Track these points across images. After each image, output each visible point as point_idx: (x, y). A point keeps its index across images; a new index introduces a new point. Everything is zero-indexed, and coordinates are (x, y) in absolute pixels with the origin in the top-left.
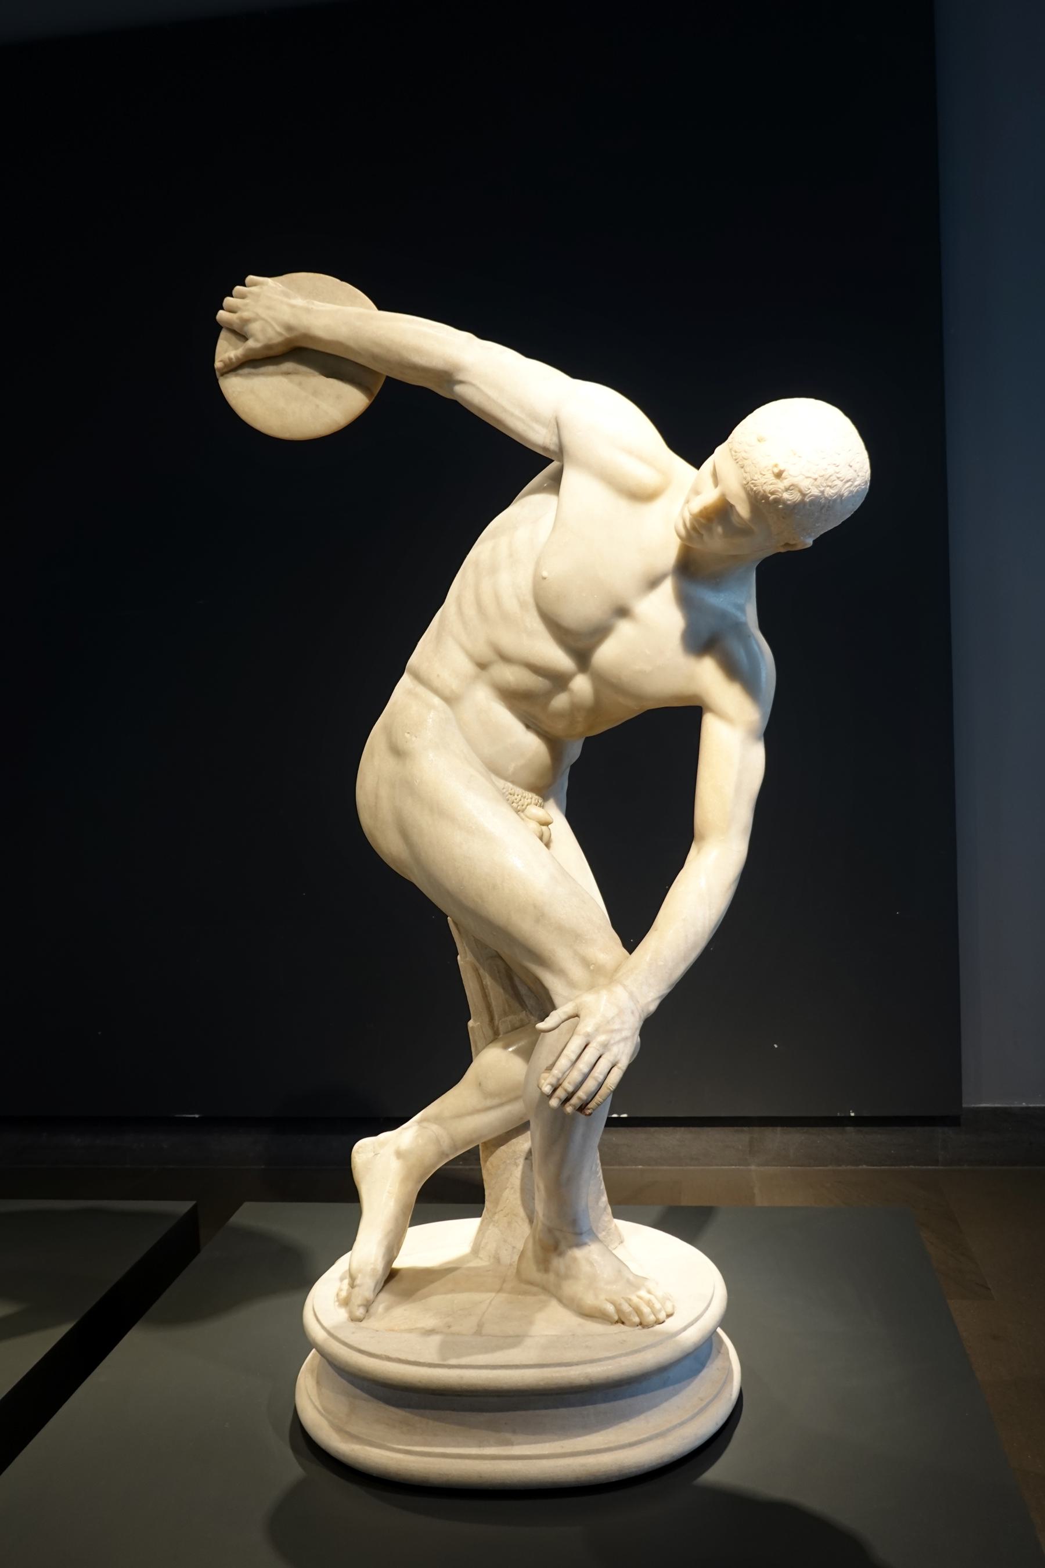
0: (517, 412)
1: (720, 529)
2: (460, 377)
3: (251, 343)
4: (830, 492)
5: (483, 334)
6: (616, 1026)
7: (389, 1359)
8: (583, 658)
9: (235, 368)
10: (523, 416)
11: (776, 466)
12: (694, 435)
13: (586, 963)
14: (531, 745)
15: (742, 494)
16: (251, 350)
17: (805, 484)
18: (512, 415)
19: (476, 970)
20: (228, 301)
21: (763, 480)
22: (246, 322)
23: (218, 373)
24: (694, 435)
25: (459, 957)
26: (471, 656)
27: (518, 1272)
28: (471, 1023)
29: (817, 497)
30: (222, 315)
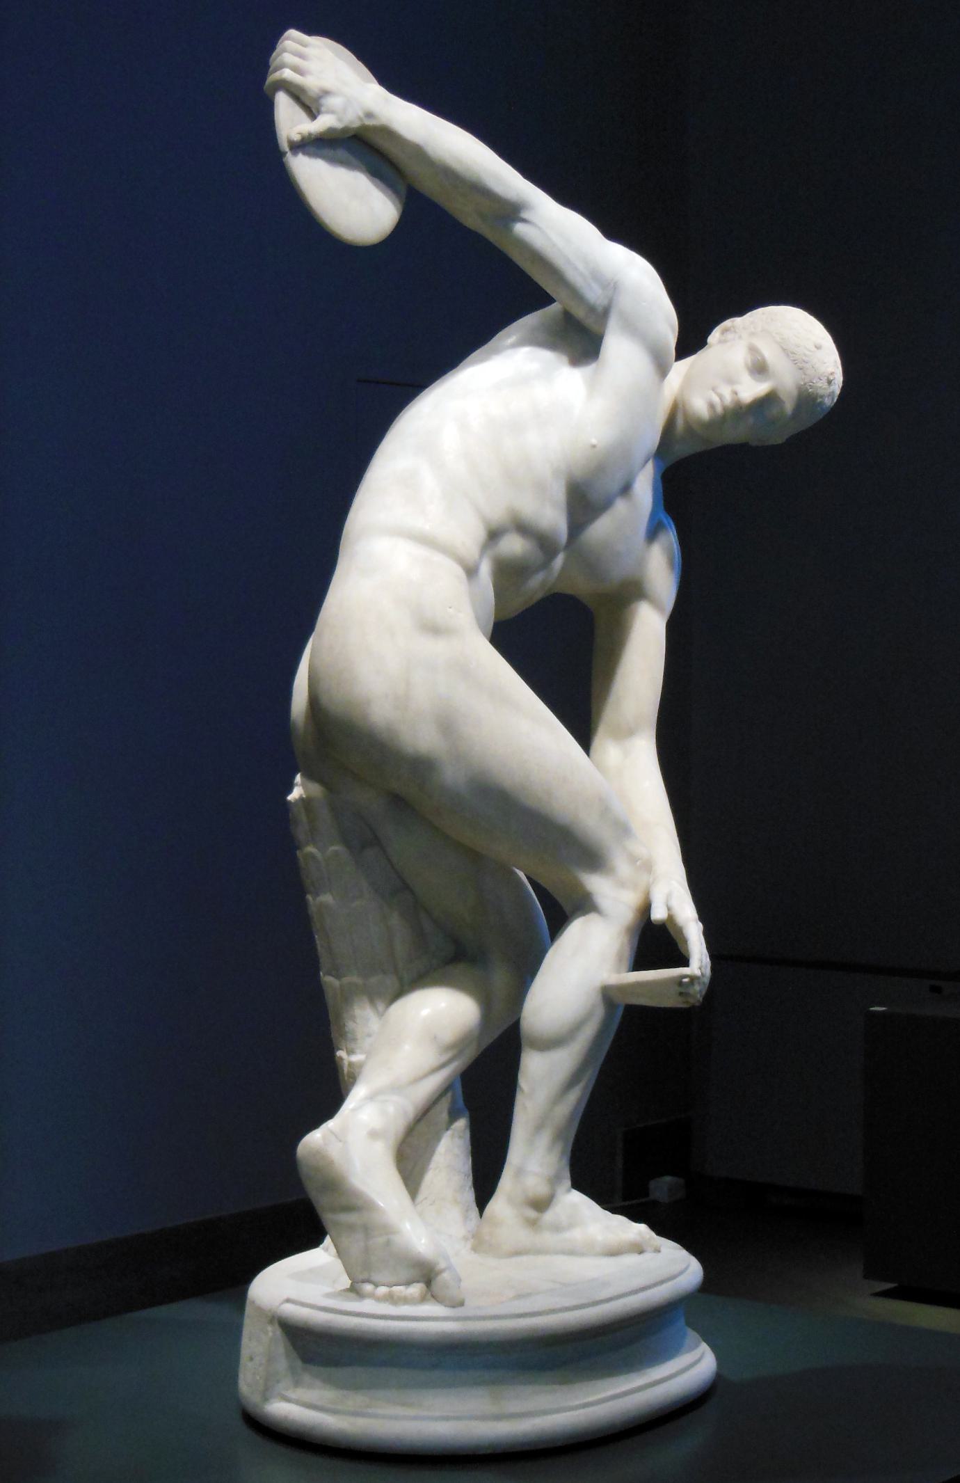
0: (581, 267)
2: (524, 215)
3: (323, 123)
11: (832, 374)
12: (698, 320)
15: (795, 393)
16: (331, 130)
18: (576, 269)
21: (819, 385)
22: (326, 93)
24: (698, 320)
26: (486, 522)
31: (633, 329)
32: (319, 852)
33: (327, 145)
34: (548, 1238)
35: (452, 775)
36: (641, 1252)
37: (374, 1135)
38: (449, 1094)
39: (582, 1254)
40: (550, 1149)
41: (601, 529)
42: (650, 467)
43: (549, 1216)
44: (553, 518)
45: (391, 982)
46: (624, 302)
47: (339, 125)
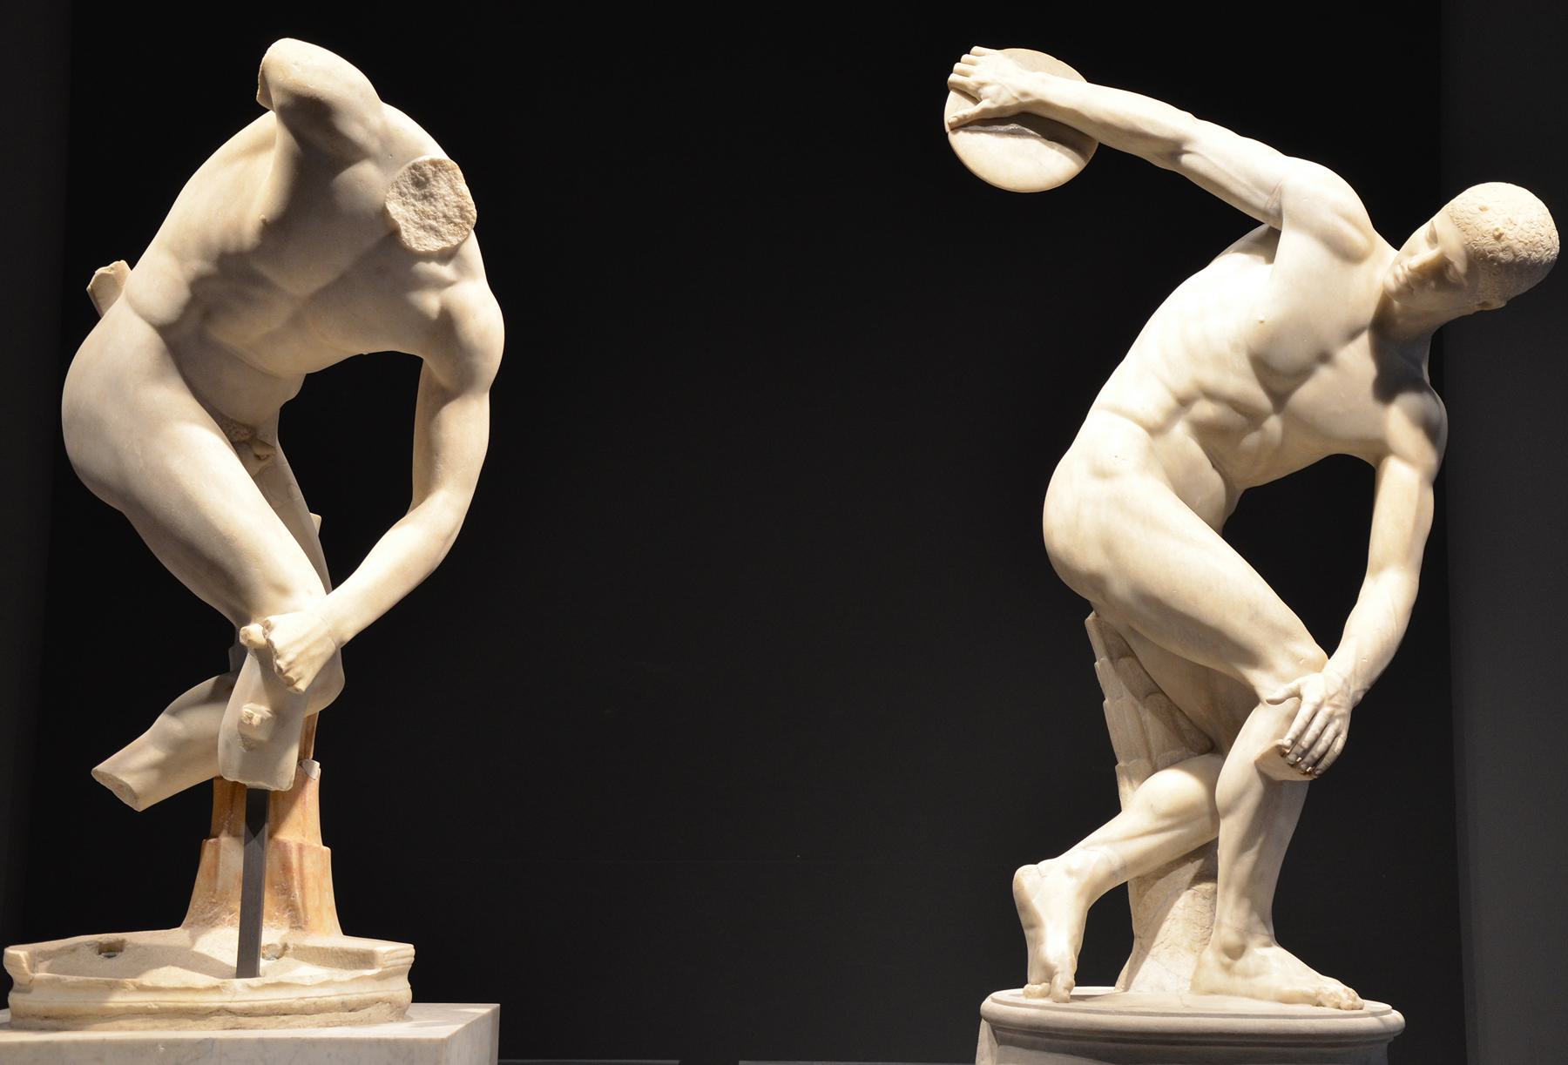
0: (1243, 180)
1: (1433, 284)
2: (1186, 148)
3: (985, 104)
4: (1535, 256)
5: (1200, 115)
6: (1335, 701)
7: (1120, 1013)
8: (1280, 399)
9: (965, 125)
10: (1249, 184)
13: (1296, 659)
14: (1214, 481)
15: (1462, 253)
16: (985, 111)
17: (1519, 246)
18: (1238, 182)
19: (1135, 707)
20: (957, 66)
22: (982, 85)
23: (947, 128)
25: (1106, 702)
27: (1195, 987)
28: (1121, 763)
29: (1525, 260)
30: (953, 78)
31: (1302, 225)
32: (1102, 664)
33: (987, 121)
34: (1238, 982)
35: (1119, 588)
36: (1319, 1004)
37: (1070, 873)
38: (1198, 863)
39: (1261, 999)
40: (1237, 904)
41: (1306, 394)
42: (1364, 340)
43: (1240, 964)
44: (1243, 384)
45: (1144, 764)
46: (1289, 204)
47: (993, 106)
